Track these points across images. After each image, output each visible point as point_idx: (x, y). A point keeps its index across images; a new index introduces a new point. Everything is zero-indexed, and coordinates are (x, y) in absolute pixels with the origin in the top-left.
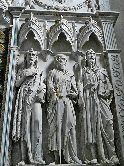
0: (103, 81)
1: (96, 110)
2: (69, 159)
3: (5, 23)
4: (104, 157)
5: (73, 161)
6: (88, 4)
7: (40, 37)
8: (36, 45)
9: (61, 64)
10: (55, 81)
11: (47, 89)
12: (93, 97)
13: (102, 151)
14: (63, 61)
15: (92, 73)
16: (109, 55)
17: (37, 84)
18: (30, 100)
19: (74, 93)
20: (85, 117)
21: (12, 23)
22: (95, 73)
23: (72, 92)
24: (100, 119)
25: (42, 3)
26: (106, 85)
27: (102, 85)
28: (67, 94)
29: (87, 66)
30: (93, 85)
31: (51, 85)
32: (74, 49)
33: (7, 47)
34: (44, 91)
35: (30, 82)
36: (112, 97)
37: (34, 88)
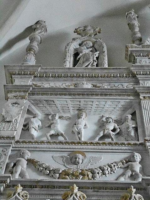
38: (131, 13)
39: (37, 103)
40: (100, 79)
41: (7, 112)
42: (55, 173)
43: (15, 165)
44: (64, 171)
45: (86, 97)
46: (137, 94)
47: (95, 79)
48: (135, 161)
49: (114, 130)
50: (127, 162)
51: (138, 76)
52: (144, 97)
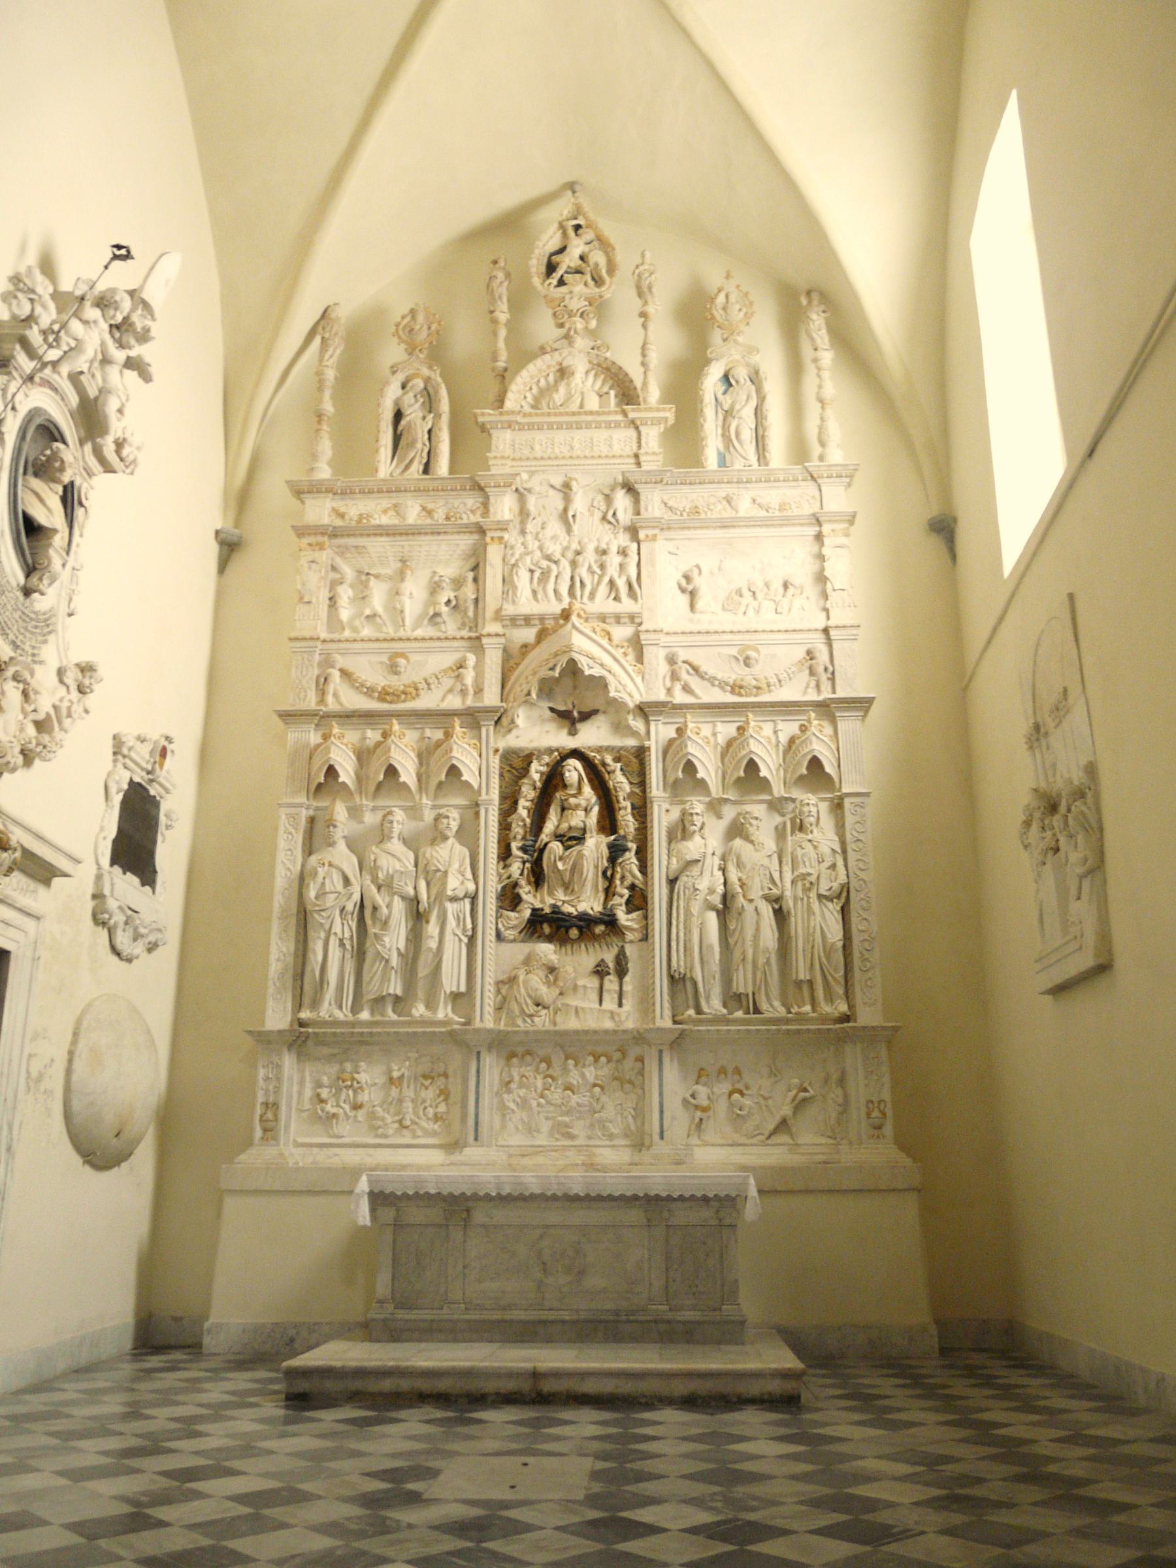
0: (830, 864)
1: (812, 924)
2: (764, 1006)
3: (634, 734)
4: (823, 1004)
5: (771, 1009)
6: (807, 664)
7: (708, 769)
8: (702, 785)
9: (751, 829)
10: (740, 865)
11: (725, 884)
12: (809, 898)
13: (820, 993)
14: (754, 822)
15: (808, 846)
16: (847, 802)
17: (707, 874)
18: (695, 908)
19: (775, 891)
20: (793, 933)
21: (648, 732)
22: (815, 847)
23: (771, 889)
24: (819, 940)
25: (706, 674)
26: (834, 874)
27: (825, 873)
28: (761, 893)
29: (801, 828)
30: (809, 874)
31: (733, 875)
32: (778, 790)
33: (644, 791)
34: (720, 889)
35: (695, 870)
36: (844, 894)
37: (703, 885)
38: (495, 277)
39: (342, 551)
40: (432, 493)
41: (303, 584)
42: (373, 691)
43: (326, 679)
44: (383, 688)
45: (410, 537)
46: (481, 531)
47: (425, 493)
48: (466, 668)
49: (448, 602)
50: (458, 668)
51: (487, 490)
52: (492, 538)
